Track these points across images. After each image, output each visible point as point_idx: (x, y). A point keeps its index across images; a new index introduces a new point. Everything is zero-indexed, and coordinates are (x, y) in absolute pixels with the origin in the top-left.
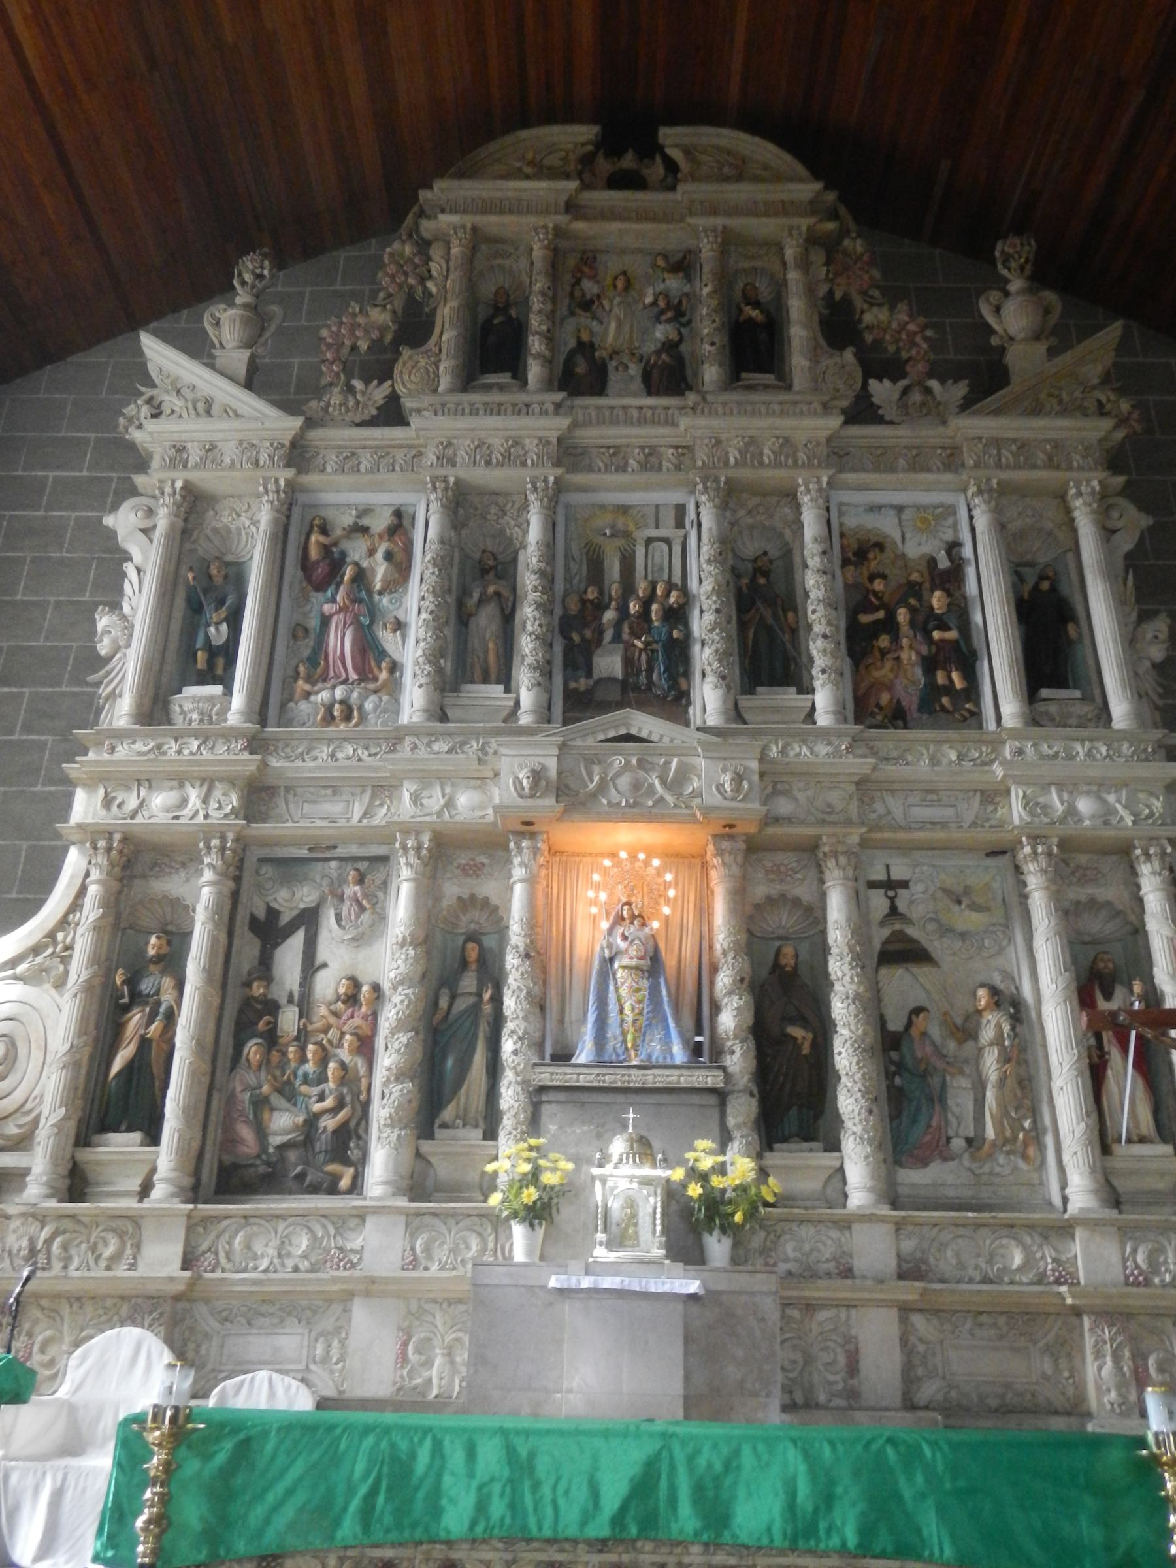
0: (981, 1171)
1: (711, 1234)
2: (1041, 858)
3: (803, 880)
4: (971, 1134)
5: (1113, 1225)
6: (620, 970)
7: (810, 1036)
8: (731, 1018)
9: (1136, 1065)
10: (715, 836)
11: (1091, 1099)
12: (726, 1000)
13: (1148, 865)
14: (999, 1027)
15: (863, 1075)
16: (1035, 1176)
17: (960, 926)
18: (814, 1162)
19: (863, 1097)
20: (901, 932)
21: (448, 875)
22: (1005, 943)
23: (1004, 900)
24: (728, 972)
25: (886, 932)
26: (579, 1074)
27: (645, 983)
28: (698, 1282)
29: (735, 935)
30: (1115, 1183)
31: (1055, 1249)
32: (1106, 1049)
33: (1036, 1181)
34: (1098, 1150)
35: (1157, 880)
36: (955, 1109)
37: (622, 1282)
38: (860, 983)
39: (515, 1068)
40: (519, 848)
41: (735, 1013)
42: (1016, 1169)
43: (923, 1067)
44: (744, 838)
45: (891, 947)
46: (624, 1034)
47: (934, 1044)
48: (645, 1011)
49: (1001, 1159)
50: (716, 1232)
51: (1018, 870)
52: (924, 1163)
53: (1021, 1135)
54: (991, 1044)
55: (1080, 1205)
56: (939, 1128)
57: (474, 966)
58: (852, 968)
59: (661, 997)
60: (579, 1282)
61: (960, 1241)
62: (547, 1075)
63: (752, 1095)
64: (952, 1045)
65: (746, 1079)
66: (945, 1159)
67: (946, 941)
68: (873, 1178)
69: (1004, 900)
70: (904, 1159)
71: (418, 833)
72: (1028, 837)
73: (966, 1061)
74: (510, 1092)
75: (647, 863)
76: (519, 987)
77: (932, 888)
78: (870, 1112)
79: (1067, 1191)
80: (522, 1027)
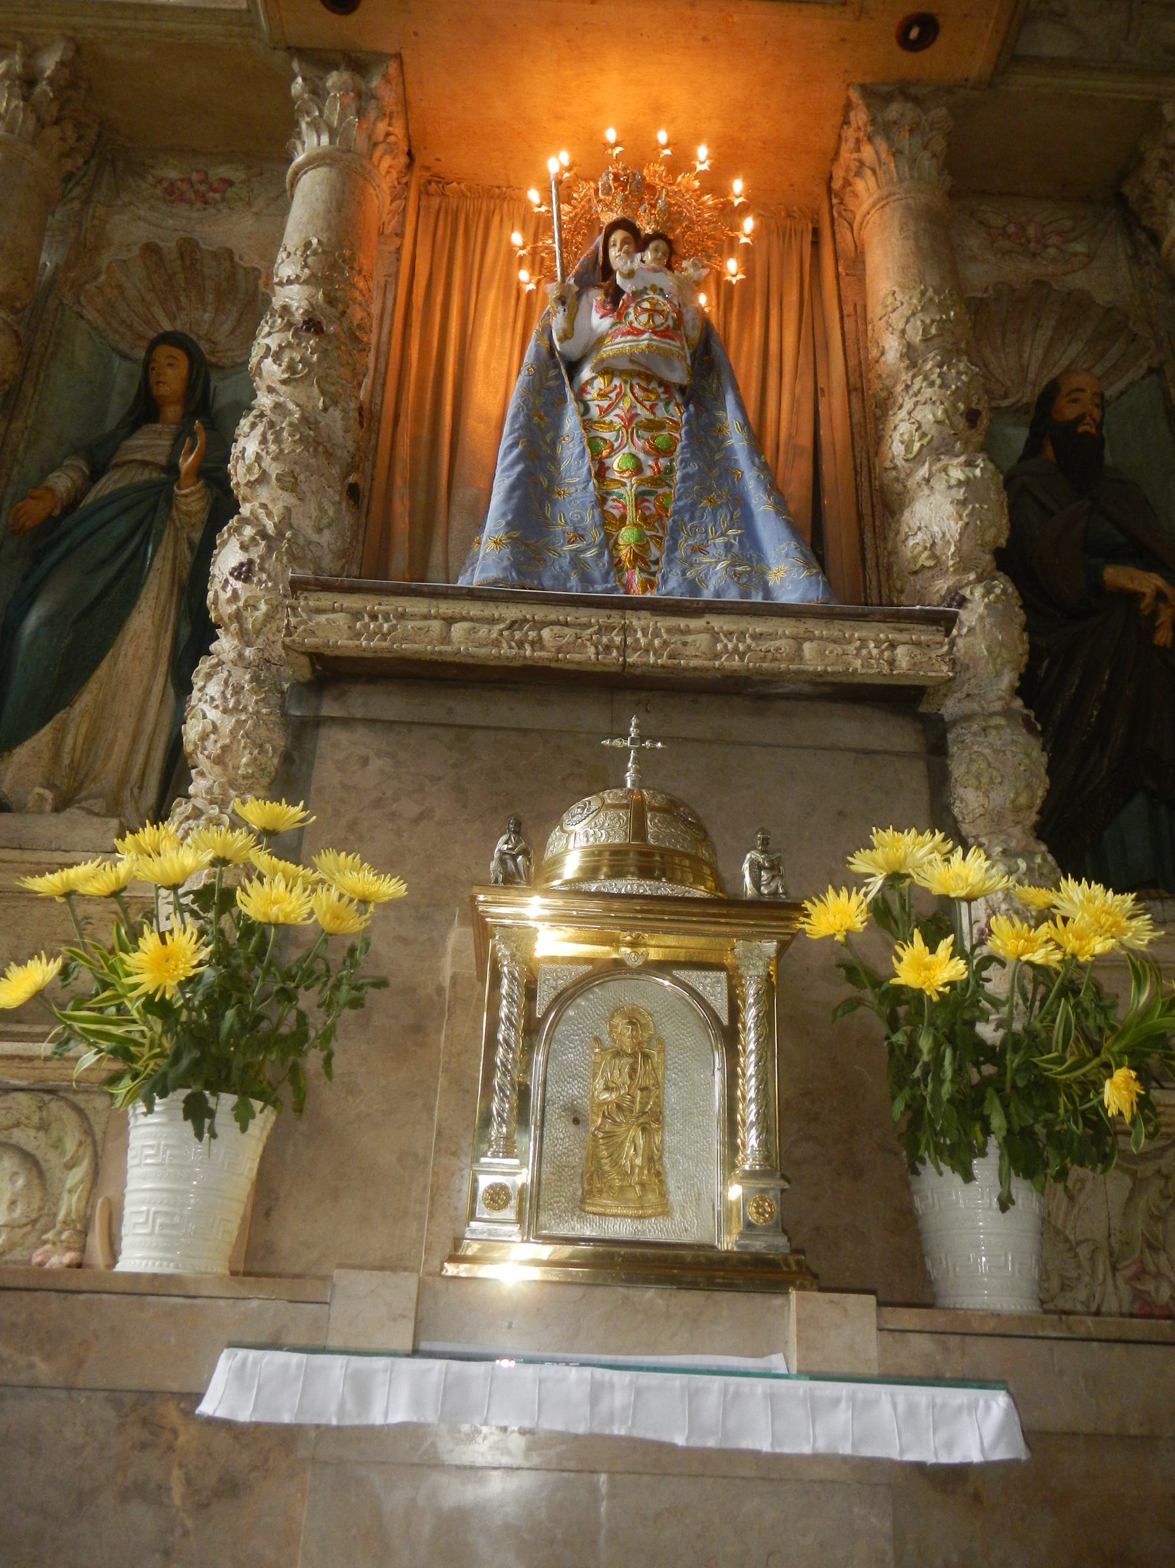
1: (968, 1177)
3: (1090, 257)
6: (600, 383)
8: (950, 509)
10: (868, 92)
12: (923, 471)
21: (125, 197)
24: (928, 393)
26: (450, 621)
27: (676, 413)
28: (999, 1402)
29: (942, 308)
37: (596, 1393)
39: (238, 616)
40: (317, 93)
41: (960, 494)
46: (609, 523)
48: (678, 475)
50: (986, 1168)
57: (172, 412)
59: (730, 451)
60: (361, 1389)
62: (341, 619)
63: (1030, 728)
71: (32, 53)
74: (213, 689)
75: (680, 162)
76: (277, 406)
80: (277, 509)
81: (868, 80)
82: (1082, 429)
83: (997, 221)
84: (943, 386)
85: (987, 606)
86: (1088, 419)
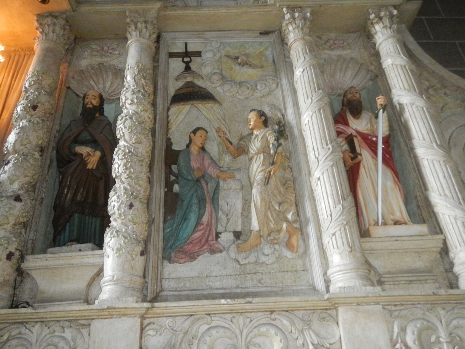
0: (247, 261)
2: (298, 21)
4: (239, 229)
5: (377, 304)
7: (98, 154)
9: (385, 161)
11: (346, 184)
13: (381, 25)
14: (265, 138)
15: (129, 177)
16: (300, 262)
17: (239, 79)
18: (75, 261)
19: (125, 193)
20: (191, 82)
22: (274, 86)
23: (274, 61)
25: (180, 84)
30: (375, 263)
31: (318, 335)
32: (358, 150)
33: (299, 268)
34: (356, 233)
35: (388, 32)
36: (226, 208)
38: (139, 103)
42: (279, 258)
43: (197, 174)
44: (64, 16)
45: (182, 92)
47: (212, 159)
49: (267, 250)
51: (283, 41)
52: (192, 257)
53: (284, 226)
54: (258, 153)
55: (340, 284)
56: (209, 224)
58: (134, 93)
61: (214, 332)
64: (227, 158)
65: (16, 186)
66: (213, 252)
67: (227, 87)
68: (123, 270)
69: (274, 61)
70: (173, 255)
72: (288, 7)
73: (239, 170)
77: (218, 55)
78: (131, 206)
79: (329, 272)
81: (39, 12)
82: (88, 106)
83: (94, 47)
84: (27, 99)
85: (13, 165)
86: (89, 103)
